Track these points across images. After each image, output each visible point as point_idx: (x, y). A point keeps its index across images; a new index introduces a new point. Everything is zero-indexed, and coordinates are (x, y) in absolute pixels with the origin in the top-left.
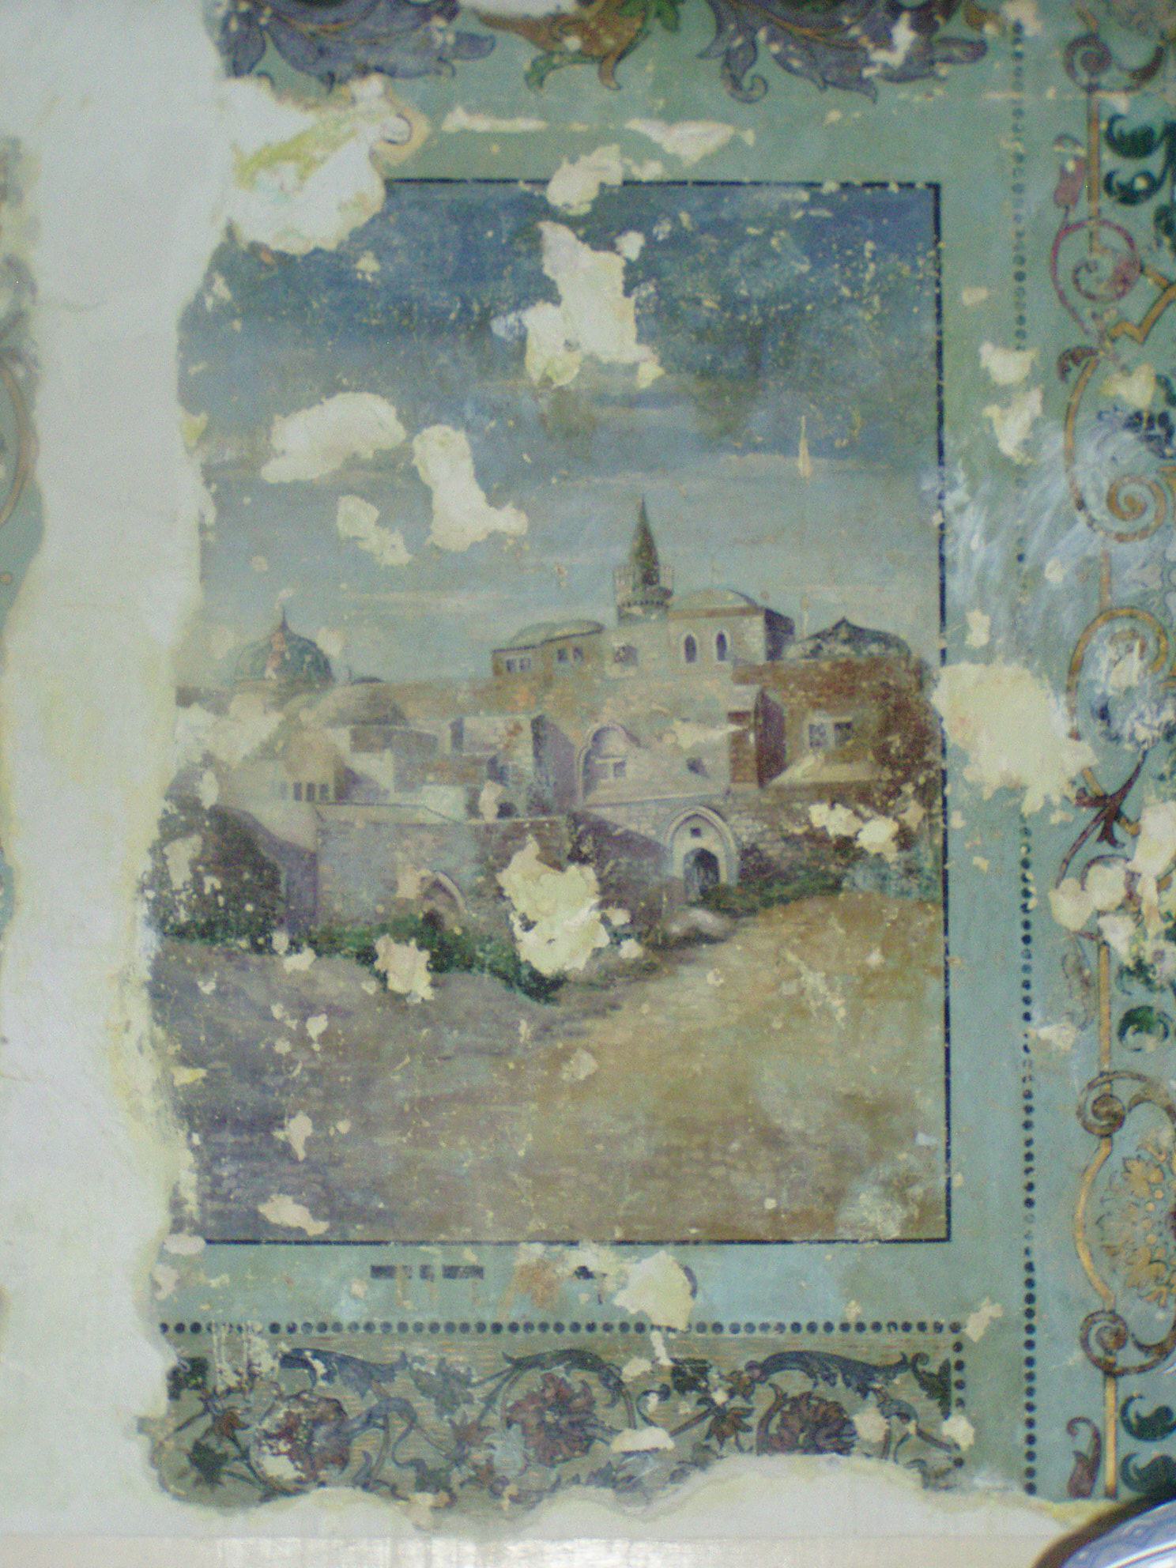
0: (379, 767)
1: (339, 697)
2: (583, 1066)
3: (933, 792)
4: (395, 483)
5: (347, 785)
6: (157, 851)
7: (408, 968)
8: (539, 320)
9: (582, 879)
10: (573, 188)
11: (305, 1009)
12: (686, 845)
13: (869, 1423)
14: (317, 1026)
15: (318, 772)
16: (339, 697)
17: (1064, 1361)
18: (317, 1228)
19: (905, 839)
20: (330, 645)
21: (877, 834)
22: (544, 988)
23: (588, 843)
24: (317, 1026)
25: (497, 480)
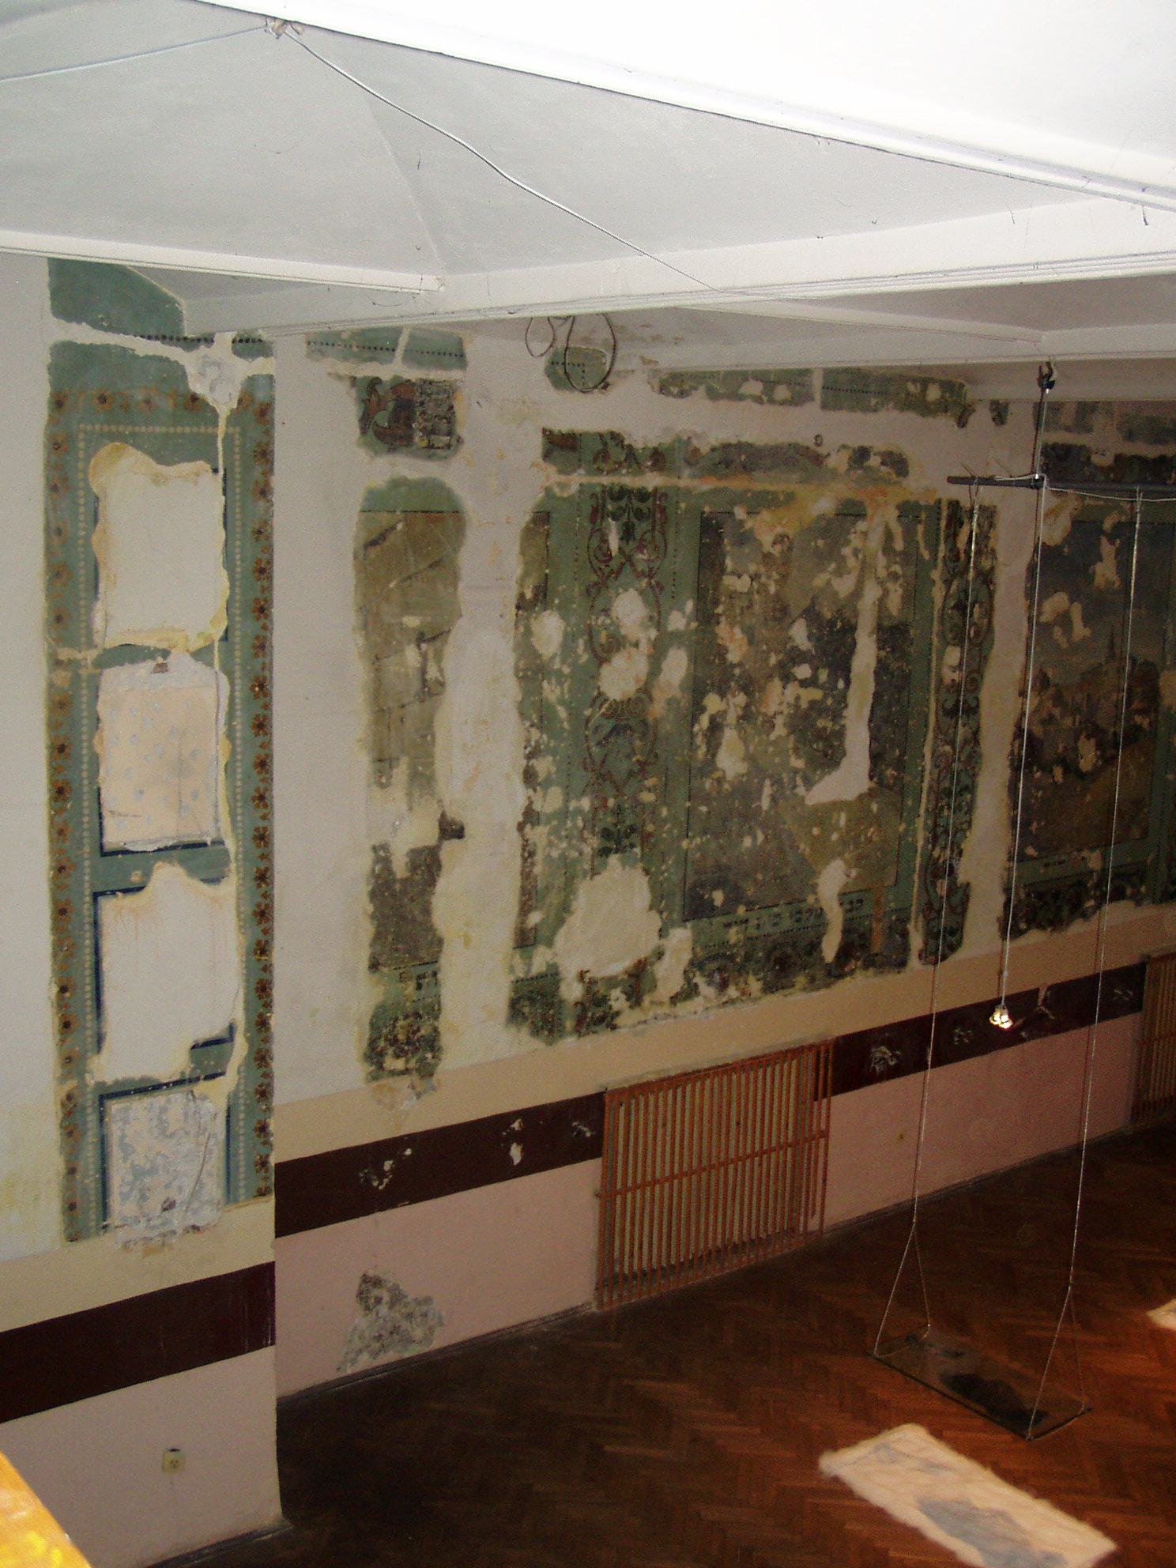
0: (1057, 712)
1: (1051, 690)
2: (1088, 798)
3: (1156, 711)
4: (1064, 620)
5: (1051, 716)
6: (1012, 745)
7: (1058, 772)
8: (1099, 568)
9: (1093, 741)
10: (1107, 525)
11: (1038, 789)
12: (1112, 730)
13: (1129, 891)
14: (1040, 794)
15: (1044, 715)
16: (1051, 690)
17: (1163, 867)
18: (1035, 854)
19: (1150, 724)
20: (1050, 674)
21: (1146, 723)
22: (1081, 775)
23: (1095, 732)
24: (1040, 794)
25: (1087, 620)
